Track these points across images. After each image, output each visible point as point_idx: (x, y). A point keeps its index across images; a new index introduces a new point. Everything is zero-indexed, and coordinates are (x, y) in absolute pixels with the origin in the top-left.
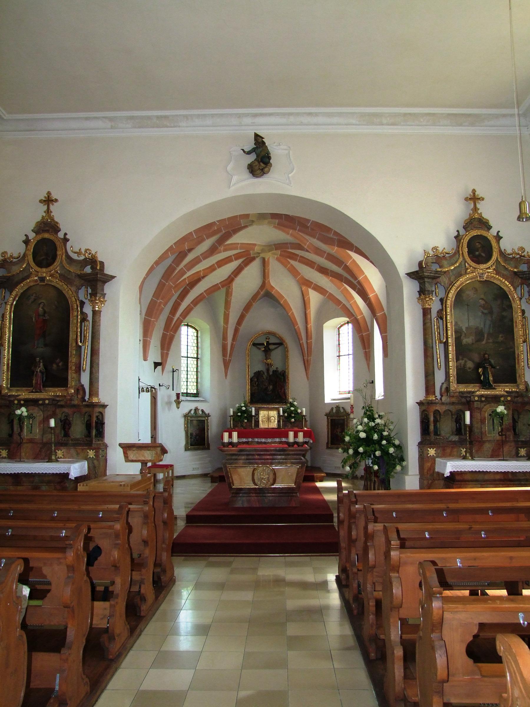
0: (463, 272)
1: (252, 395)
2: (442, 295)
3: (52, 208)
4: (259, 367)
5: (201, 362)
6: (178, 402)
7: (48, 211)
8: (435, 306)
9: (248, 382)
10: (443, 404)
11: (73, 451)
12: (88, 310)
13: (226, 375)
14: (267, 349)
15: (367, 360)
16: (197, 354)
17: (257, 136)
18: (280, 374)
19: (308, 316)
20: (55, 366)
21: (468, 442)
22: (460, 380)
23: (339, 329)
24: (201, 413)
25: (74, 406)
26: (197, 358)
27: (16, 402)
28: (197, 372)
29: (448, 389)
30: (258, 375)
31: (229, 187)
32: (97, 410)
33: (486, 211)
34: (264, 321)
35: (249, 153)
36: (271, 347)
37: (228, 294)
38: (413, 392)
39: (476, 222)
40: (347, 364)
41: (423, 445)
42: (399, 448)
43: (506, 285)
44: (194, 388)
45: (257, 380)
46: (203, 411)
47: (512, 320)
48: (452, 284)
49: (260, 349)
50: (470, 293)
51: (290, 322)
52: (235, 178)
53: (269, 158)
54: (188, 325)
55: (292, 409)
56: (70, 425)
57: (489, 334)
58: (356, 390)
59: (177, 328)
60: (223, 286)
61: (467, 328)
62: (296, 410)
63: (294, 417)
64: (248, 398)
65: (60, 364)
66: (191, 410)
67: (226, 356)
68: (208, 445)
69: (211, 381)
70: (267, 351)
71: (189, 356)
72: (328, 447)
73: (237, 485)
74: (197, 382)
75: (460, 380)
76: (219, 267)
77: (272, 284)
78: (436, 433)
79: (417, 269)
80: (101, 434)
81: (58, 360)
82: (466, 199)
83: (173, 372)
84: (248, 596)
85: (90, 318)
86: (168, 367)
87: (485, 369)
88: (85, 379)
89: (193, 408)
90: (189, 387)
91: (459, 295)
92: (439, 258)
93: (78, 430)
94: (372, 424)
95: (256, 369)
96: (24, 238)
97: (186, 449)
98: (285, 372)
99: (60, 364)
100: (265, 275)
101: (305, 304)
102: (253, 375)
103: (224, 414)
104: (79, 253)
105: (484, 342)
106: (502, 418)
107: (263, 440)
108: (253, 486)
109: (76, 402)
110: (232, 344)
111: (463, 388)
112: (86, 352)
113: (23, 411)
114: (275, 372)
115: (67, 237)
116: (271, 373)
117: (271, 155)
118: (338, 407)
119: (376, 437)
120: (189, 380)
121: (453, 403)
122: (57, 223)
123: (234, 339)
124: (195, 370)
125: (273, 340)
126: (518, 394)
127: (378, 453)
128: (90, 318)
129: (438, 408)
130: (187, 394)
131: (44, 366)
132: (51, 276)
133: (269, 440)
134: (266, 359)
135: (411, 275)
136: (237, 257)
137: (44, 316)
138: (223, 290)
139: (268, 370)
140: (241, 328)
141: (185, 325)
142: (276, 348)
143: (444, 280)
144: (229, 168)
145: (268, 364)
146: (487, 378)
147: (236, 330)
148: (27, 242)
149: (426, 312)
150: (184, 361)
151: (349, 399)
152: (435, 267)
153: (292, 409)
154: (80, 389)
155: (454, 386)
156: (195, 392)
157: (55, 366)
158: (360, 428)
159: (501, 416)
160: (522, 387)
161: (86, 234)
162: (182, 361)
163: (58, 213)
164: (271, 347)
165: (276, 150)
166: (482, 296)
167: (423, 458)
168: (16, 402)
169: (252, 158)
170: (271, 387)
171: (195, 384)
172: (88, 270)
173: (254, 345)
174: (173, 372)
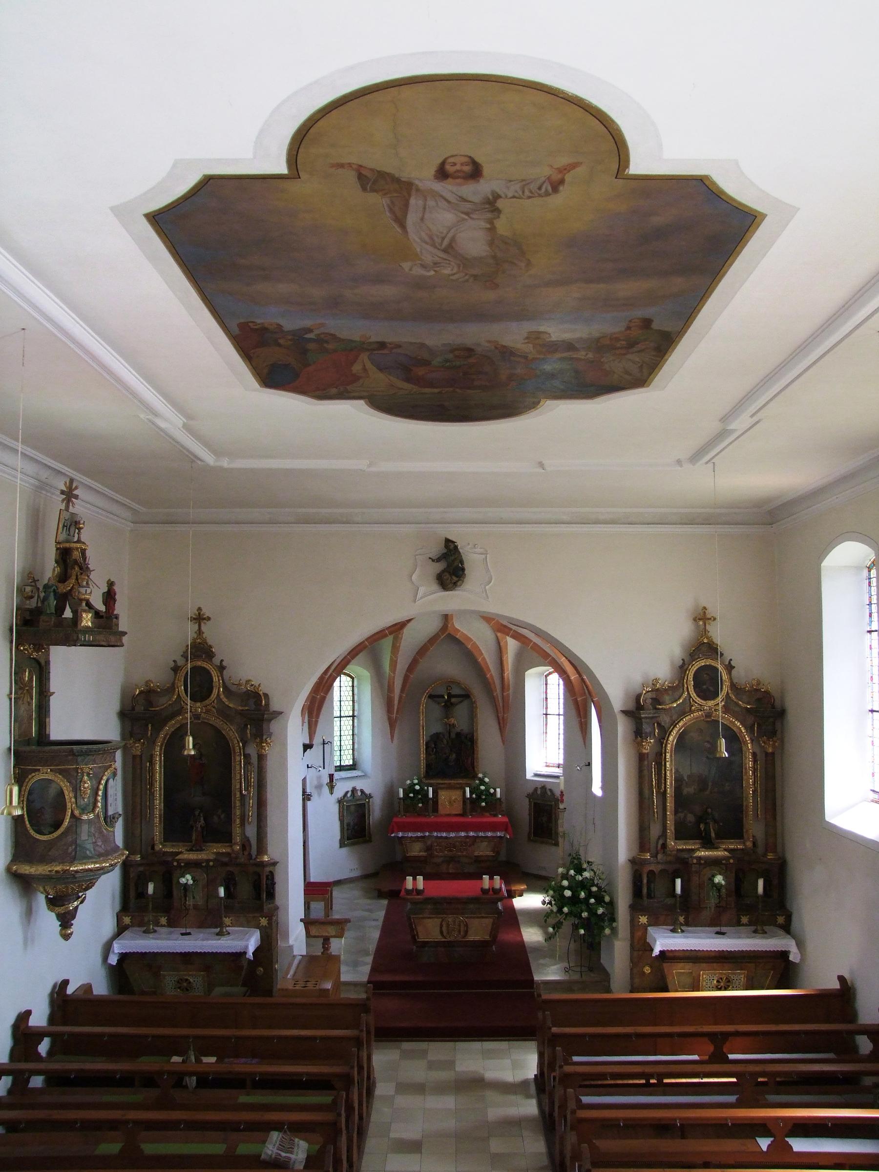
0: (687, 709)
1: (428, 766)
3: (203, 628)
4: (437, 728)
5: (359, 720)
6: (331, 786)
7: (200, 632)
9: (423, 748)
12: (252, 750)
16: (353, 710)
17: (448, 541)
19: (505, 663)
20: (216, 819)
21: (685, 913)
22: (678, 836)
23: (546, 676)
24: (359, 793)
27: (175, 864)
28: (353, 735)
29: (664, 846)
31: (415, 601)
32: (268, 869)
33: (718, 634)
35: (438, 560)
36: (453, 700)
40: (556, 726)
41: (635, 908)
42: (611, 905)
44: (350, 757)
45: (434, 742)
46: (362, 791)
48: (674, 724)
49: (439, 703)
52: (422, 590)
53: (463, 569)
55: (483, 788)
58: (567, 766)
60: (391, 633)
61: (689, 777)
62: (487, 790)
63: (484, 800)
65: (222, 816)
66: (347, 792)
68: (370, 838)
72: (529, 839)
73: (422, 938)
74: (353, 750)
75: (678, 836)
77: (457, 626)
80: (271, 895)
81: (220, 811)
82: (695, 620)
84: (449, 1102)
85: (254, 760)
88: (251, 831)
89: (350, 789)
90: (344, 757)
91: (681, 737)
93: (244, 889)
95: (434, 731)
96: (172, 664)
97: (342, 845)
98: (473, 736)
99: (222, 816)
101: (500, 651)
102: (429, 739)
103: (390, 792)
105: (708, 792)
106: (719, 890)
107: (444, 834)
108: (440, 938)
109: (242, 860)
113: (187, 879)
114: (458, 735)
115: (224, 664)
116: (453, 735)
117: (466, 566)
118: (544, 788)
119: (583, 895)
120: (344, 748)
121: (670, 862)
122: (211, 647)
124: (351, 733)
125: (456, 691)
127: (585, 914)
128: (254, 760)
130: (340, 768)
131: (205, 820)
132: (208, 712)
133: (452, 835)
134: (447, 717)
135: (625, 712)
137: (200, 758)
144: (414, 577)
151: (557, 777)
153: (483, 788)
155: (671, 843)
156: (351, 763)
158: (565, 883)
159: (718, 887)
160: (749, 844)
165: (471, 557)
166: (708, 739)
167: (633, 923)
168: (175, 864)
170: (454, 756)
171: (351, 752)
173: (431, 697)
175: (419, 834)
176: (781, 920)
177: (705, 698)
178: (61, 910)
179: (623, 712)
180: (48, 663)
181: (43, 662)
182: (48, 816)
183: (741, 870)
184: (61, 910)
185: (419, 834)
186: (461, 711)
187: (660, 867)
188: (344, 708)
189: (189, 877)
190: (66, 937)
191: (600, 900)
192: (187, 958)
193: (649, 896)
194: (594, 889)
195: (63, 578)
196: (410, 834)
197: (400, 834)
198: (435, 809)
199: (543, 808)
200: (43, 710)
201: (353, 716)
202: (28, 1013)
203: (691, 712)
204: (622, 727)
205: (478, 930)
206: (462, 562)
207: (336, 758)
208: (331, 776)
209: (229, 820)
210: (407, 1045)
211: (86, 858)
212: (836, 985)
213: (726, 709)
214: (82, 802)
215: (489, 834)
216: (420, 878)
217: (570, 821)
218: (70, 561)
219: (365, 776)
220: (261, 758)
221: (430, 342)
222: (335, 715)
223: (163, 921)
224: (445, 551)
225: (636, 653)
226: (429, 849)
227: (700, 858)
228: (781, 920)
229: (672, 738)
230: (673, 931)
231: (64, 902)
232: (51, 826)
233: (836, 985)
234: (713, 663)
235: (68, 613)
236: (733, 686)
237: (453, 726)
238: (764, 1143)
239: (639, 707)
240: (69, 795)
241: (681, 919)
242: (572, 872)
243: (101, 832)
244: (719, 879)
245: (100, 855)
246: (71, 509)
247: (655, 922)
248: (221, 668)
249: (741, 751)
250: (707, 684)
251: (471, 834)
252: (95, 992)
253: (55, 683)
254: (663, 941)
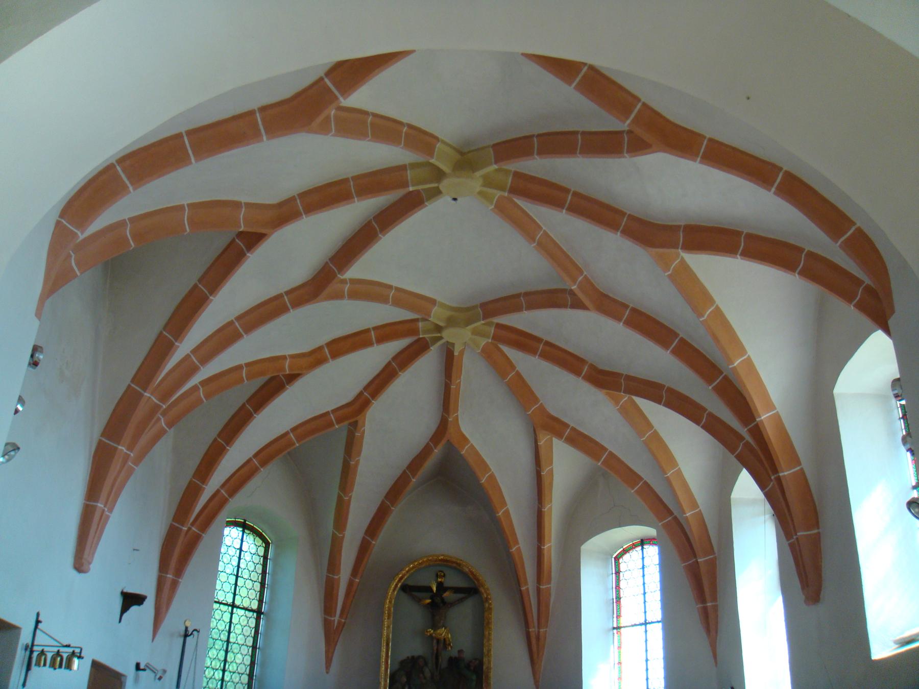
4: (415, 648)
5: (268, 621)
14: (438, 600)
15: (708, 630)
16: (261, 601)
18: (468, 666)
23: (617, 559)
26: (259, 612)
28: (254, 647)
34: (433, 534)
37: (352, 445)
49: (419, 600)
54: (244, 526)
59: (209, 518)
60: (339, 421)
71: (237, 602)
76: (335, 355)
77: (466, 429)
83: (186, 635)
86: (174, 621)
98: (481, 663)
100: (447, 400)
102: (397, 667)
114: (454, 662)
116: (444, 664)
120: (231, 667)
124: (250, 642)
125: (452, 580)
134: (435, 627)
136: (386, 333)
138: (341, 430)
140: (377, 543)
141: (235, 524)
142: (461, 601)
145: (438, 641)
147: (364, 549)
150: (220, 615)
162: (217, 615)
174: (186, 635)
188: (243, 592)
201: (259, 612)
222: (220, 596)
237: (445, 643)
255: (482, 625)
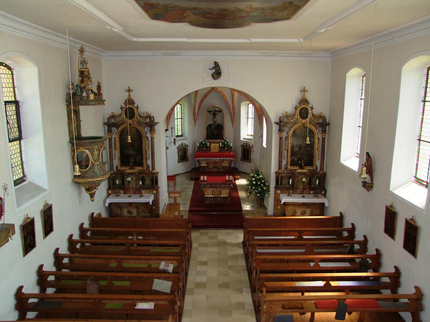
1: (207, 135)
2: (288, 131)
4: (211, 122)
8: (284, 135)
10: (284, 173)
11: (148, 191)
12: (149, 135)
13: (195, 125)
17: (215, 63)
20: (138, 158)
21: (292, 189)
22: (292, 165)
25: (146, 173)
29: (287, 168)
30: (210, 126)
32: (156, 175)
33: (309, 96)
35: (212, 69)
36: (216, 113)
38: (274, 168)
39: (304, 101)
40: (251, 121)
41: (276, 188)
42: (268, 186)
43: (313, 128)
44: (181, 132)
45: (209, 128)
46: (185, 144)
47: (314, 142)
50: (298, 131)
51: (226, 102)
52: (206, 80)
53: (221, 73)
55: (226, 143)
56: (145, 180)
57: (304, 147)
62: (227, 144)
63: (226, 147)
64: (205, 137)
67: (195, 116)
68: (188, 159)
69: (189, 129)
70: (214, 115)
72: (241, 160)
75: (292, 165)
78: (281, 184)
79: (278, 121)
80: (157, 183)
82: (301, 91)
84: (215, 249)
87: (301, 161)
88: (149, 162)
91: (294, 132)
92: (287, 116)
93: (148, 182)
94: (258, 177)
95: (209, 123)
96: (121, 107)
97: (179, 162)
101: (233, 96)
103: (194, 144)
104: (144, 114)
106: (304, 183)
109: (147, 172)
110: (198, 112)
111: (292, 168)
112: (149, 152)
113: (129, 179)
114: (218, 124)
116: (216, 125)
118: (246, 143)
119: (259, 183)
123: (199, 109)
126: (313, 170)
127: (260, 189)
128: (150, 139)
129: (282, 175)
130: (177, 136)
131: (134, 159)
133: (216, 159)
134: (214, 119)
135: (276, 123)
139: (215, 124)
143: (289, 125)
146: (301, 164)
147: (200, 106)
148: (122, 108)
149: (281, 139)
150: (176, 121)
151: (251, 140)
152: (286, 120)
153: (226, 143)
154: (148, 167)
155: (289, 167)
157: (138, 158)
158: (253, 179)
159: (304, 182)
160: (315, 168)
161: (146, 105)
163: (133, 96)
164: (216, 113)
169: (214, 71)
172: (148, 120)
173: (208, 111)
175: (204, 159)
176: (323, 192)
177: (303, 119)
178: (91, 192)
179: (275, 123)
180: (79, 110)
181: (77, 110)
182: (84, 163)
183: (312, 176)
184: (91, 192)
185: (204, 159)
186: (218, 117)
187: (285, 175)
188: (178, 116)
189: (130, 178)
190: (93, 201)
191: (265, 185)
192: (130, 204)
193: (281, 184)
194: (263, 181)
195: (82, 82)
196: (201, 159)
197: (198, 159)
198: (210, 150)
199: (246, 151)
200: (78, 127)
201: (182, 118)
202: (83, 224)
203: (298, 123)
204: (275, 128)
205: (225, 193)
206: (220, 70)
207: (176, 133)
208: (175, 139)
209: (142, 159)
210: (202, 231)
211: (97, 177)
212: (339, 215)
213: (310, 123)
214: (95, 159)
215: (228, 159)
216: (205, 177)
217: (255, 155)
218: (84, 75)
219: (186, 139)
220: (152, 138)
221: (212, 8)
223: (122, 192)
224: (214, 66)
225: (280, 103)
226: (208, 163)
227: (298, 172)
228: (323, 192)
229: (291, 132)
230: (288, 196)
231: (91, 189)
232: (85, 166)
233: (339, 215)
234: (306, 107)
235: (84, 94)
236: (313, 115)
238: (312, 264)
239: (280, 121)
240: (90, 156)
241: (291, 192)
242: (256, 176)
243: (101, 168)
244: (304, 180)
245: (102, 175)
246: (83, 57)
247: (282, 193)
248: (138, 108)
249: (314, 137)
250: (304, 113)
251: (222, 159)
252: (102, 217)
253: (82, 117)
254: (285, 199)
255: (223, 118)
